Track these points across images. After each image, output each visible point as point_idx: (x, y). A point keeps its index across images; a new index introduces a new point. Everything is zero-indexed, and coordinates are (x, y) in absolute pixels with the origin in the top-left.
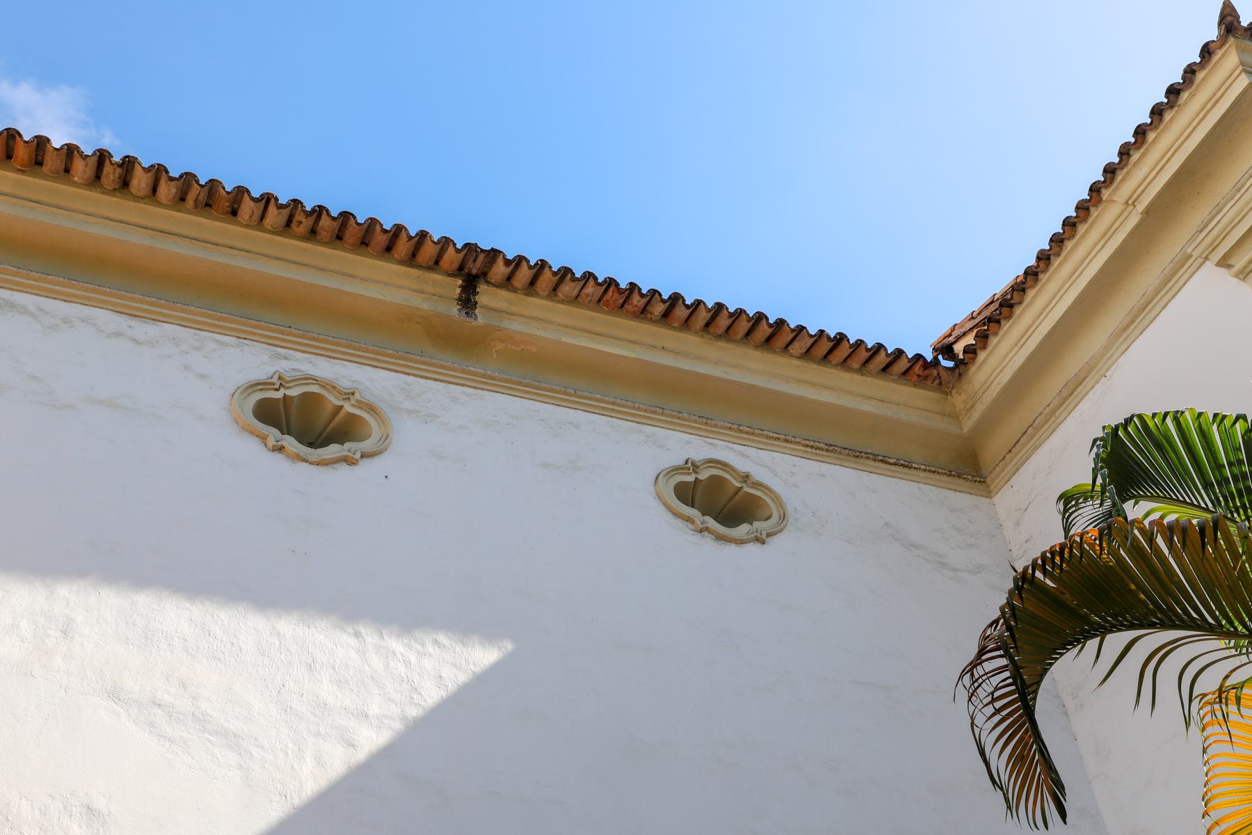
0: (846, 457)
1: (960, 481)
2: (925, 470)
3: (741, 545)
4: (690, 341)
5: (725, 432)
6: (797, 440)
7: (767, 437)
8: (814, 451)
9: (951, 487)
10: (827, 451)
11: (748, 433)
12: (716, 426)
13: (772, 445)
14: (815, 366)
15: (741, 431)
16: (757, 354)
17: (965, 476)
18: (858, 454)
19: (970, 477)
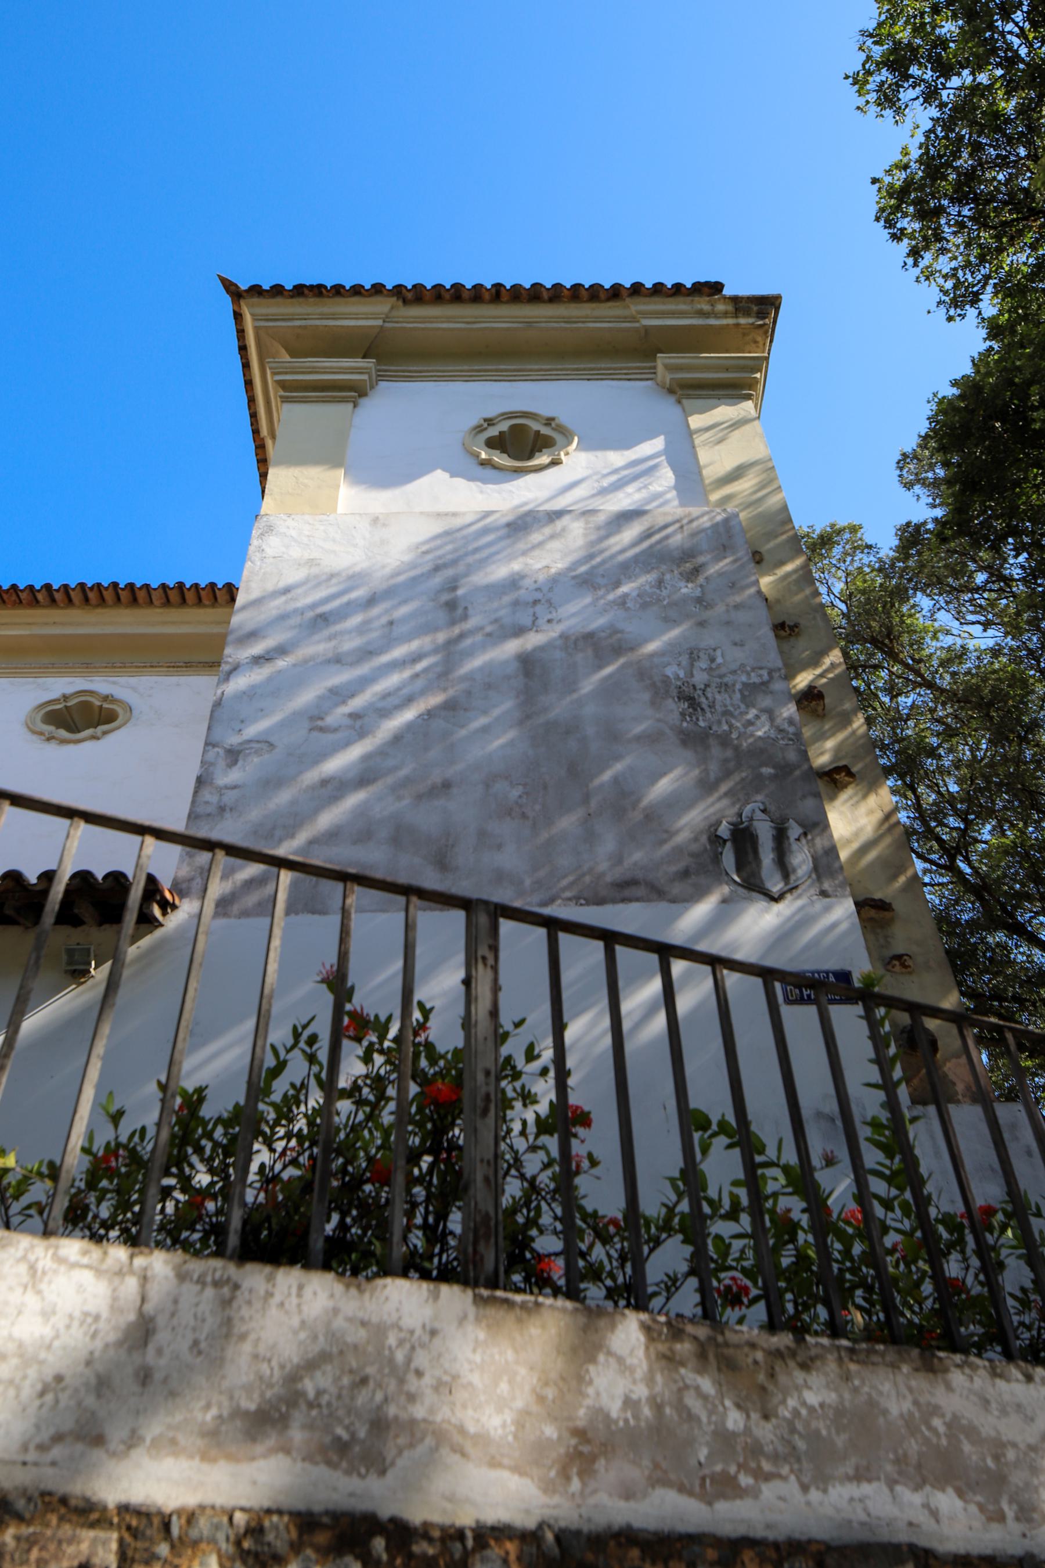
4: (75, 614)
7: (137, 667)
12: (95, 668)
16: (127, 611)
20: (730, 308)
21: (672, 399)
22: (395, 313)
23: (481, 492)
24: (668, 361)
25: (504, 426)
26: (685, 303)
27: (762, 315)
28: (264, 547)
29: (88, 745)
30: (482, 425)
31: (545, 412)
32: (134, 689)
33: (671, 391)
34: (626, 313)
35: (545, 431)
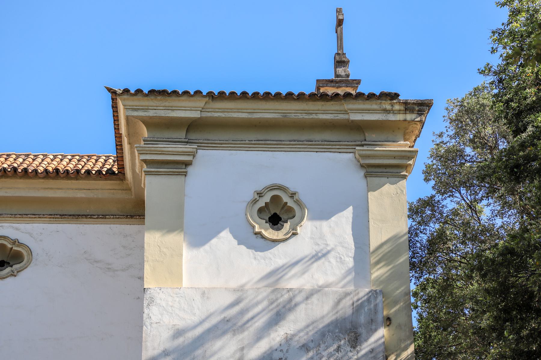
0: (72, 219)
1: (133, 220)
2: (113, 218)
3: (4, 280)
5: (9, 219)
6: (45, 216)
7: (30, 218)
8: (55, 219)
9: (128, 223)
10: (61, 218)
11: (20, 218)
12: (3, 217)
13: (33, 220)
14: (52, 180)
15: (16, 217)
17: (135, 217)
18: (77, 217)
19: (137, 217)
20: (402, 108)
21: (362, 173)
22: (208, 106)
23: (255, 258)
24: (361, 152)
25: (267, 198)
26: (376, 104)
27: (420, 113)
28: (151, 315)
29: (10, 280)
30: (256, 199)
31: (292, 189)
32: (31, 235)
33: (362, 166)
34: (341, 108)
35: (290, 203)
